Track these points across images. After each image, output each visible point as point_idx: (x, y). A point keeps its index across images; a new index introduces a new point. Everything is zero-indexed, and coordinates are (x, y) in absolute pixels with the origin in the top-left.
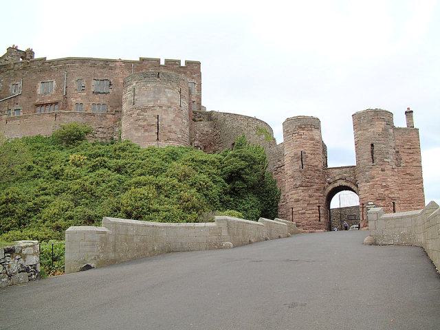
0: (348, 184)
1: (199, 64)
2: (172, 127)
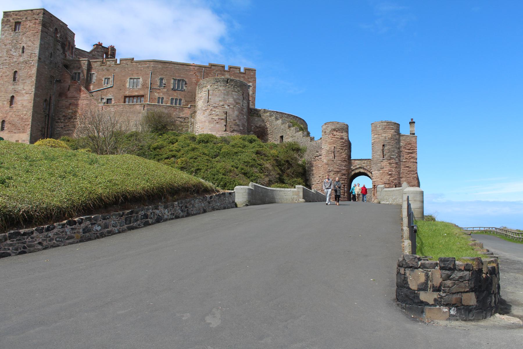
0: (366, 172)
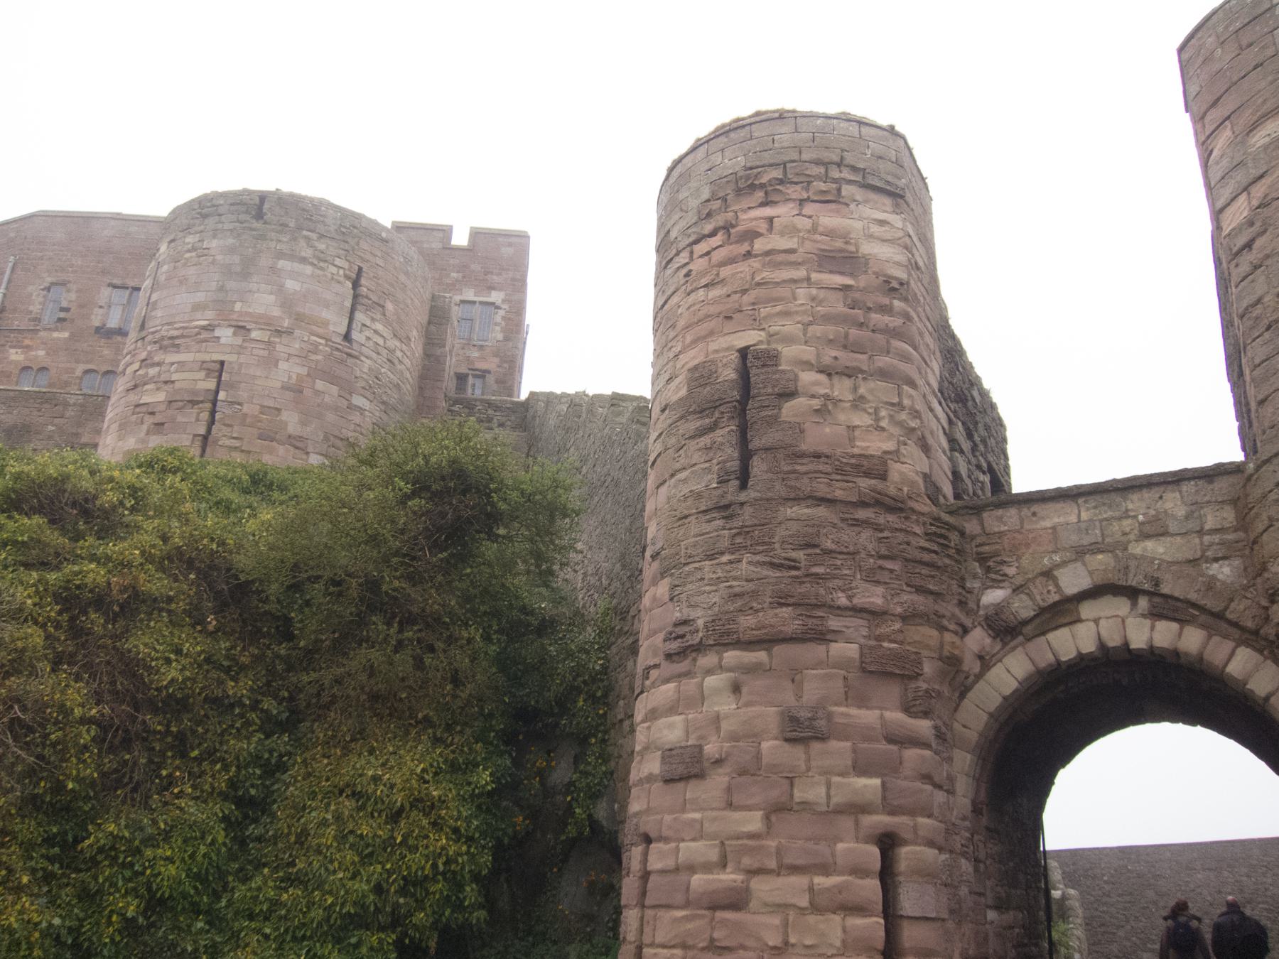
2: (285, 416)
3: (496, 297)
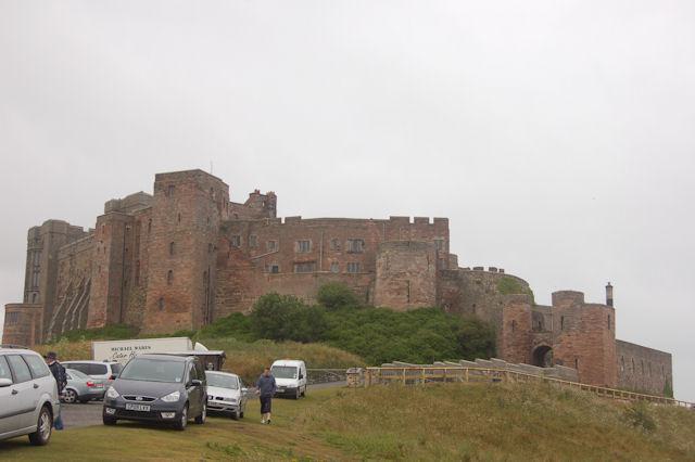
1: (446, 221)
3: (443, 238)
